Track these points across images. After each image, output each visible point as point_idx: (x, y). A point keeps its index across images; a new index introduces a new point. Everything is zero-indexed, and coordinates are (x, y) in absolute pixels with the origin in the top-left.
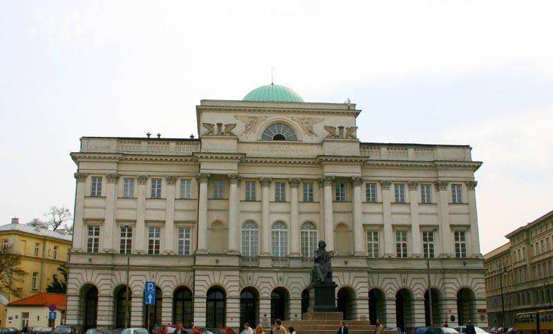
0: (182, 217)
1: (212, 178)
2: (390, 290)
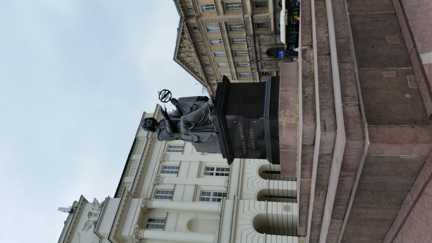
2: (260, 184)
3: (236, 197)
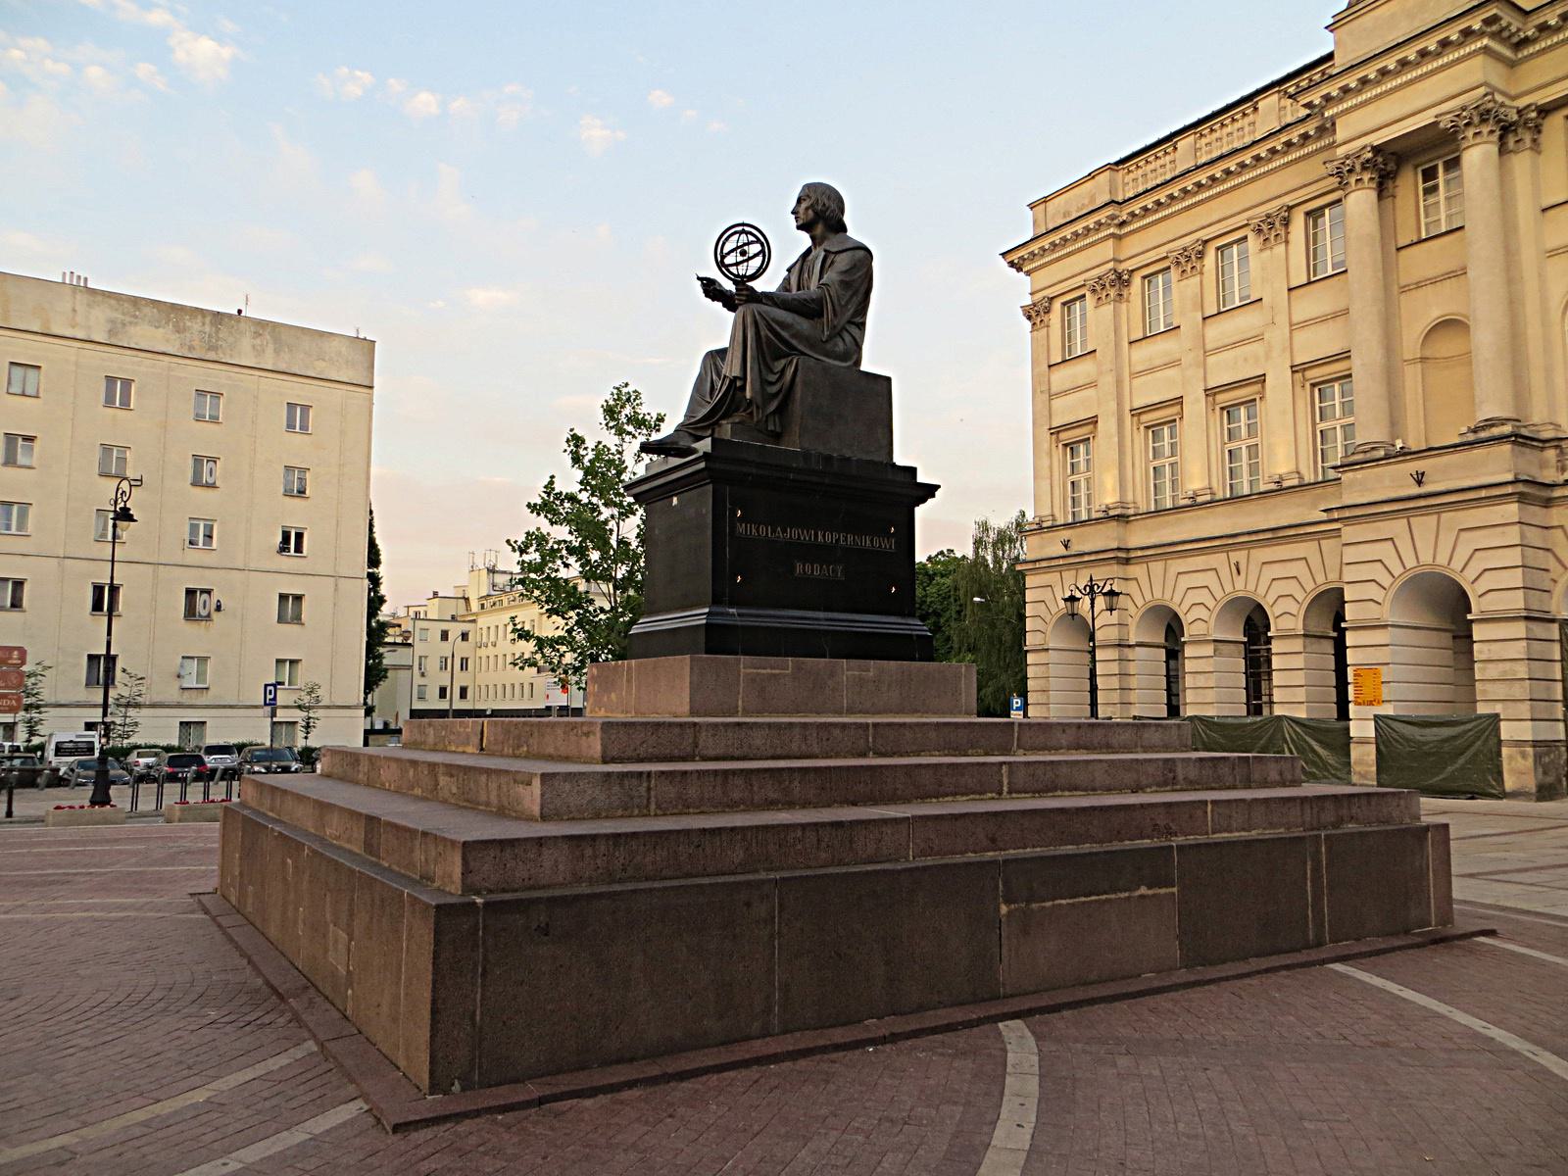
0: (1315, 344)
1: (1389, 164)
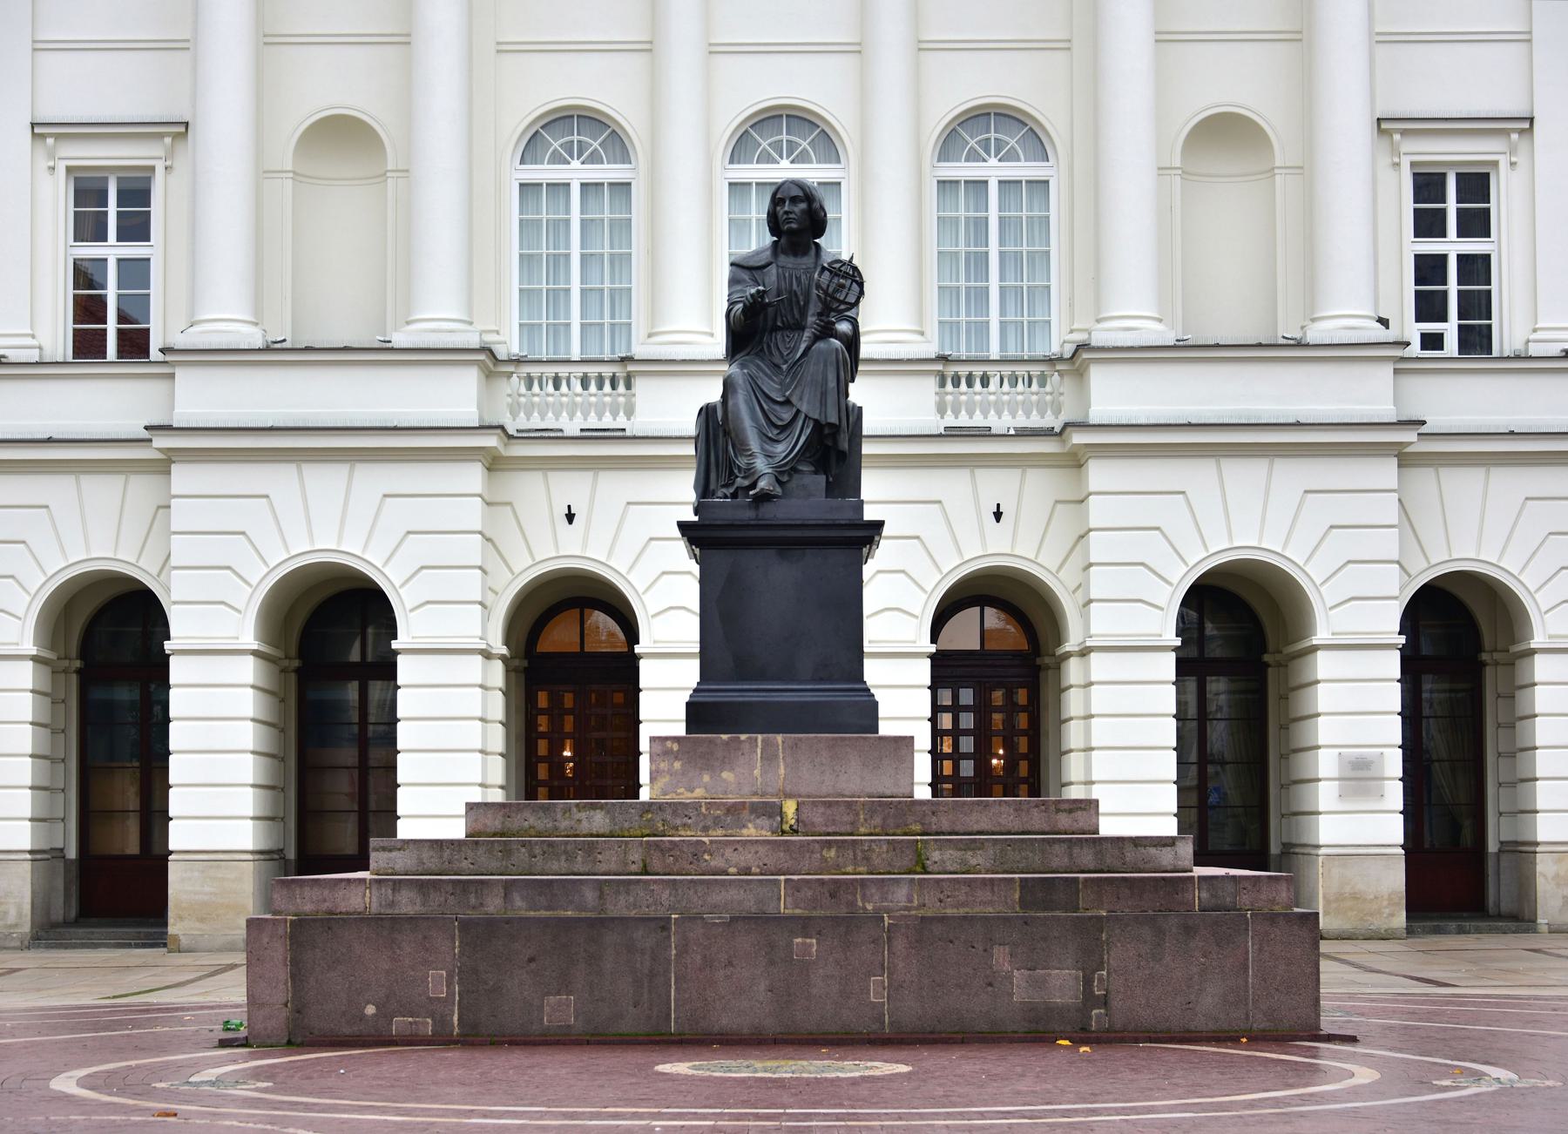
3: (1409, 436)
